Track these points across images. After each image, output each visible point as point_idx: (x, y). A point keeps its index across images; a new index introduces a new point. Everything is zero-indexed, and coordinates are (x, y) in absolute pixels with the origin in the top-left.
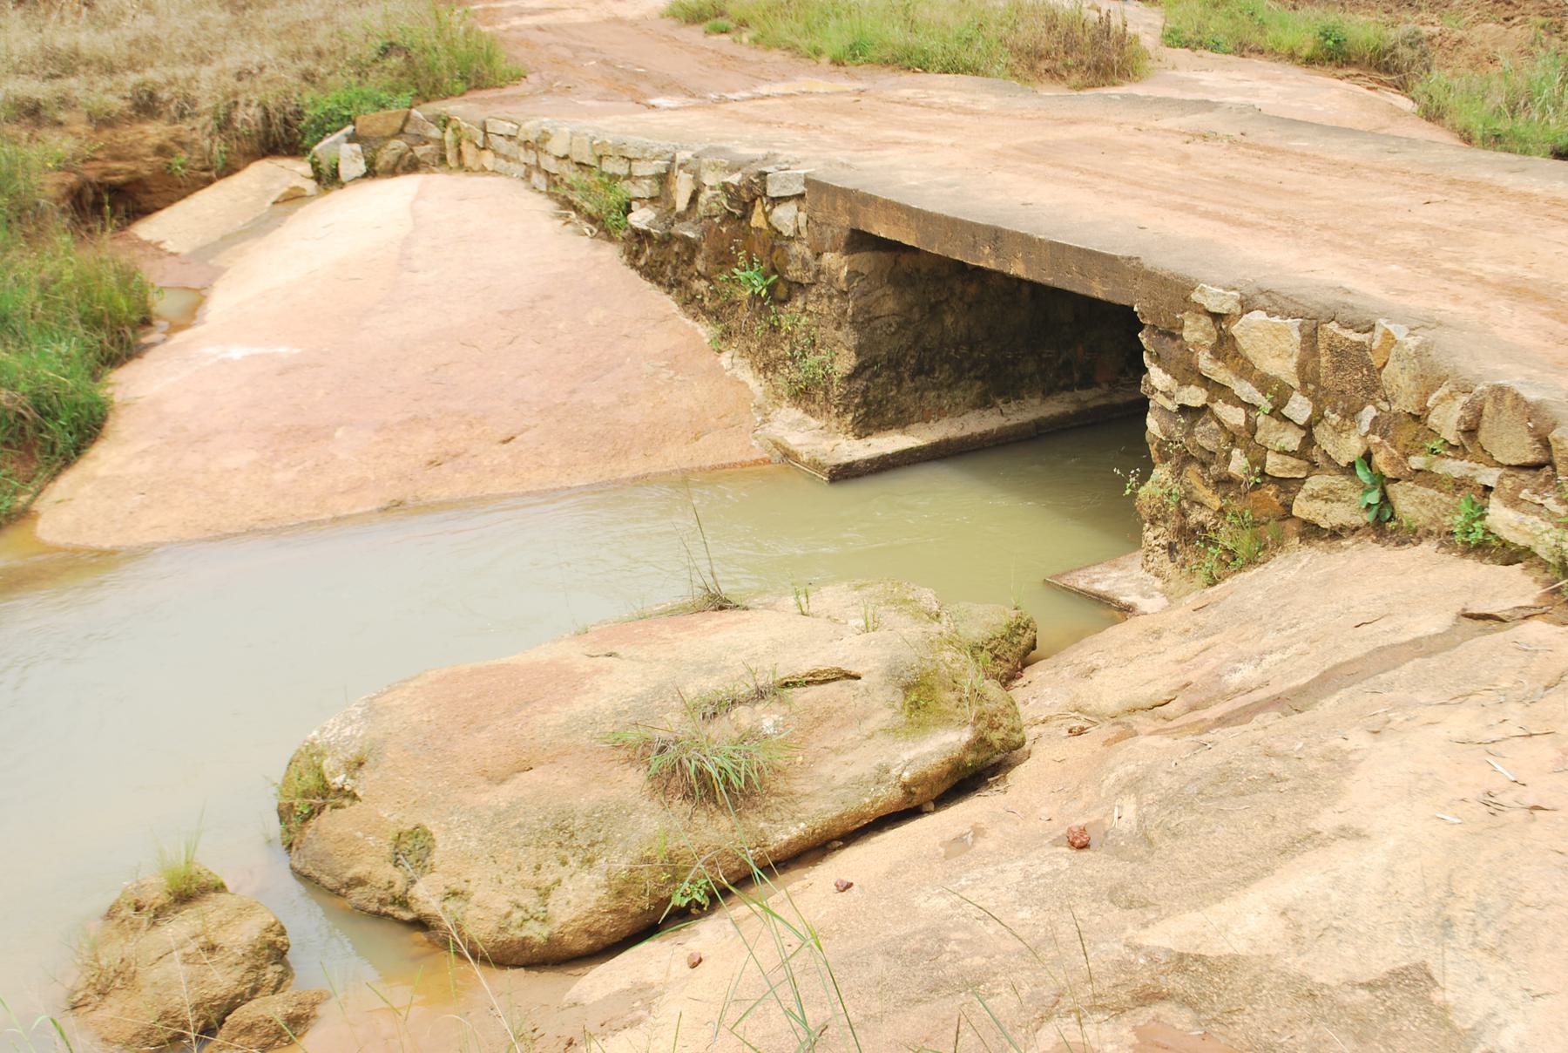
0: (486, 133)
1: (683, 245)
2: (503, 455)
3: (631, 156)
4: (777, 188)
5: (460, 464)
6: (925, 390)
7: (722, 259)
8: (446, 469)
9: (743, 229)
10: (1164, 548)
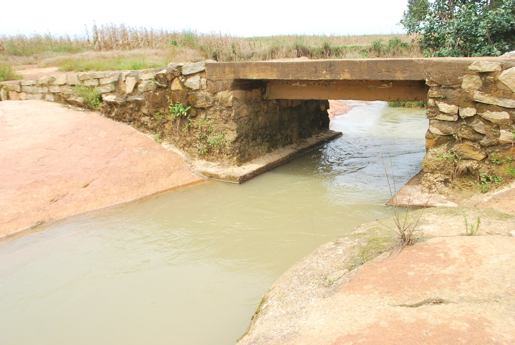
0: (21, 86)
1: (135, 105)
2: (86, 193)
3: (98, 77)
4: (188, 71)
5: (67, 199)
6: (255, 146)
7: (157, 106)
8: (60, 202)
9: (168, 92)
10: (441, 181)
